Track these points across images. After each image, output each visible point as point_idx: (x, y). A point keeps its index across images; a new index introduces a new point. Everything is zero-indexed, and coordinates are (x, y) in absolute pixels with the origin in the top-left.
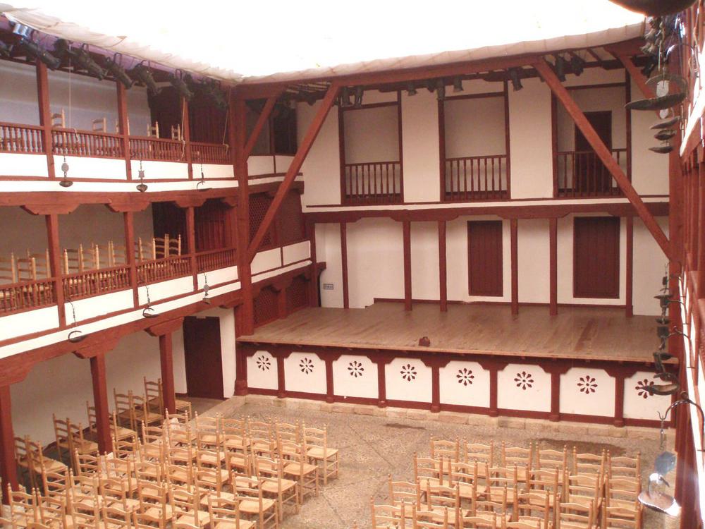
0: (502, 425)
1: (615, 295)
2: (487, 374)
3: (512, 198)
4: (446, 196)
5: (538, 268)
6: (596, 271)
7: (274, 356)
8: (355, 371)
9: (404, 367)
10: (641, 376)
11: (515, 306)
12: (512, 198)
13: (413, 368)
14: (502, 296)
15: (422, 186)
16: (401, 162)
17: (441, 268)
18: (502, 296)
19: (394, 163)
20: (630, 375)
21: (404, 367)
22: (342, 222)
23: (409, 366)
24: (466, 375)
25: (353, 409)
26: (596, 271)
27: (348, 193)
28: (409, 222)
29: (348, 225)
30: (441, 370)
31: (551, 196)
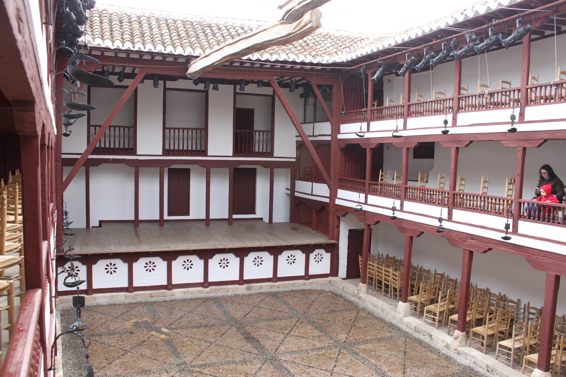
0: (248, 289)
1: (169, 214)
2: (126, 266)
3: (209, 155)
4: (166, 152)
5: (210, 197)
6: (242, 200)
7: (83, 264)
8: (151, 268)
9: (185, 262)
10: (317, 251)
11: (207, 221)
12: (209, 155)
13: (191, 261)
14: (189, 215)
15: (150, 144)
16: (134, 128)
17: (151, 198)
18: (189, 215)
19: (129, 127)
20: (312, 252)
21: (185, 262)
22: (87, 165)
23: (188, 260)
24: (111, 270)
25: (151, 294)
26: (242, 200)
27: (167, 148)
28: (138, 168)
29: (91, 168)
30: (210, 261)
31: (231, 155)
